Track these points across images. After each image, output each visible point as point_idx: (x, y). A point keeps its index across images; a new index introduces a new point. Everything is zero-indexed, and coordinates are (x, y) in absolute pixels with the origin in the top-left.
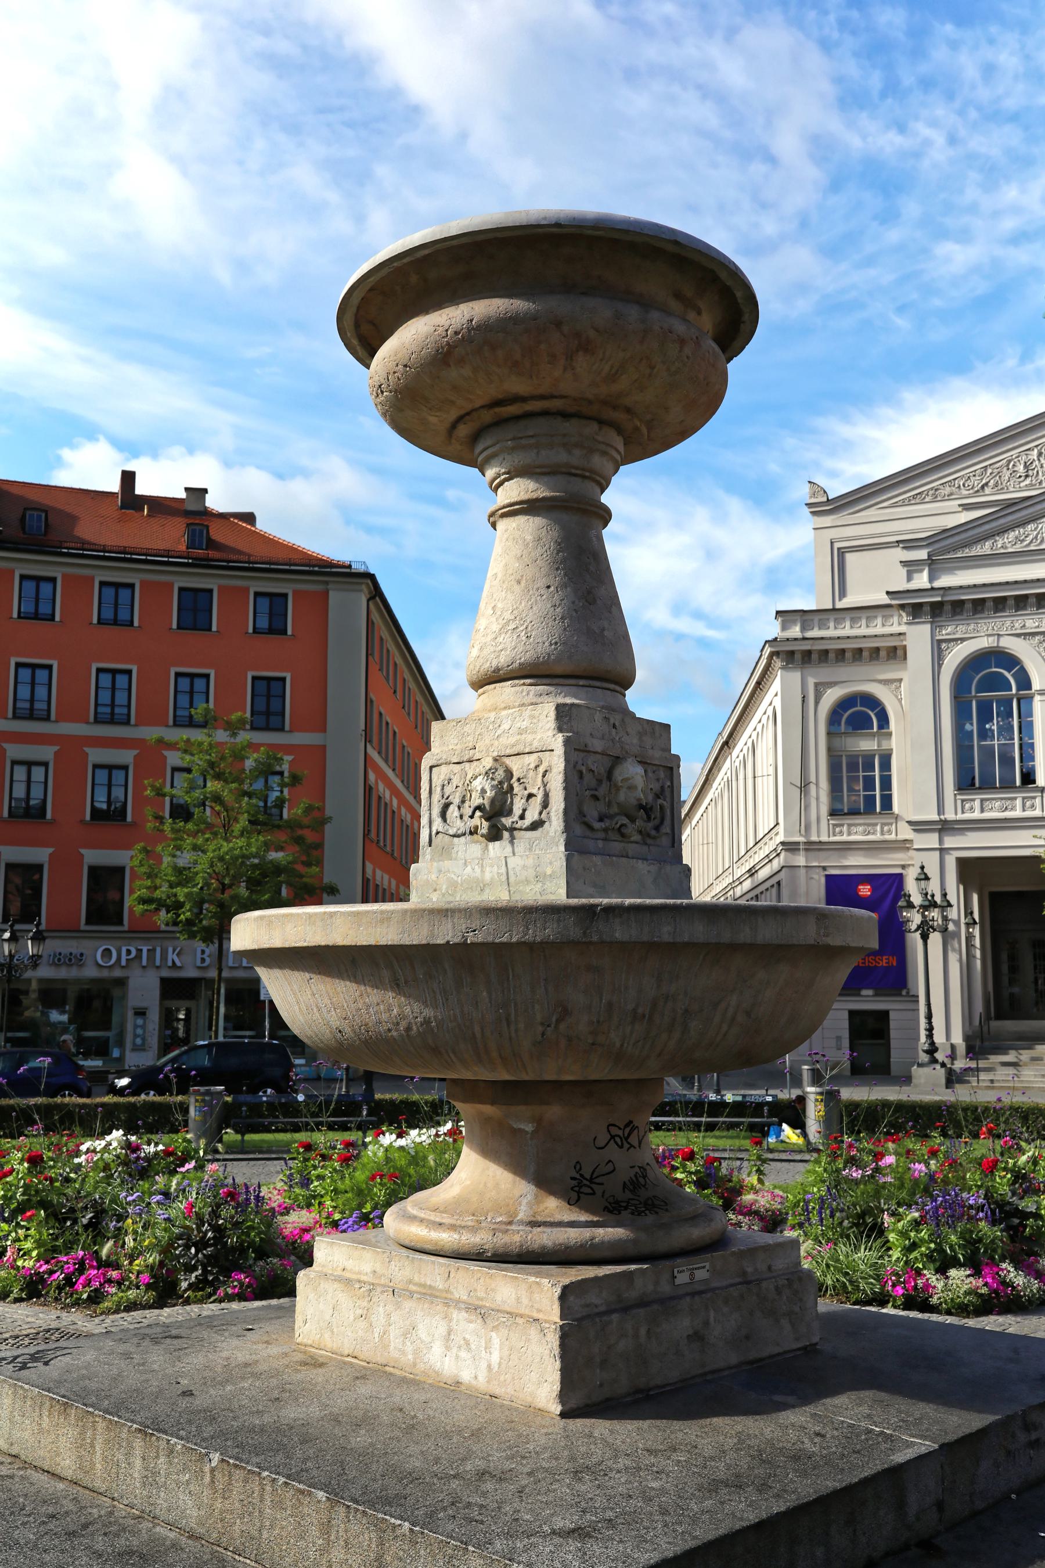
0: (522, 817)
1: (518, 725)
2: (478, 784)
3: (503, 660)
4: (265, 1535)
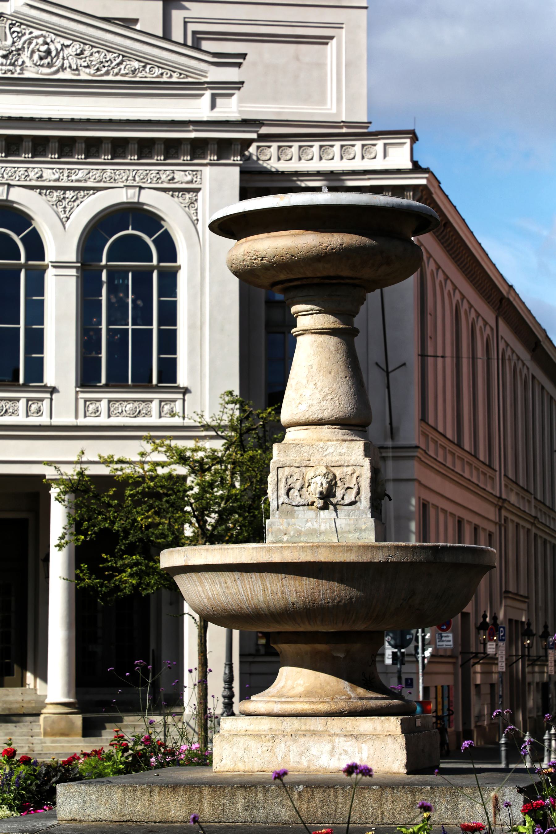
0: (343, 499)
1: (339, 451)
2: (319, 480)
3: (326, 415)
4: (339, 811)
